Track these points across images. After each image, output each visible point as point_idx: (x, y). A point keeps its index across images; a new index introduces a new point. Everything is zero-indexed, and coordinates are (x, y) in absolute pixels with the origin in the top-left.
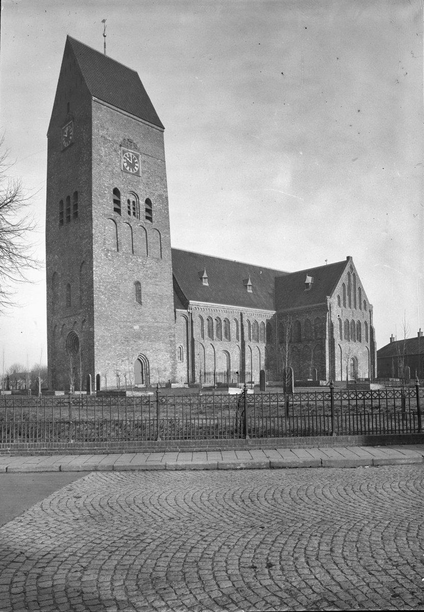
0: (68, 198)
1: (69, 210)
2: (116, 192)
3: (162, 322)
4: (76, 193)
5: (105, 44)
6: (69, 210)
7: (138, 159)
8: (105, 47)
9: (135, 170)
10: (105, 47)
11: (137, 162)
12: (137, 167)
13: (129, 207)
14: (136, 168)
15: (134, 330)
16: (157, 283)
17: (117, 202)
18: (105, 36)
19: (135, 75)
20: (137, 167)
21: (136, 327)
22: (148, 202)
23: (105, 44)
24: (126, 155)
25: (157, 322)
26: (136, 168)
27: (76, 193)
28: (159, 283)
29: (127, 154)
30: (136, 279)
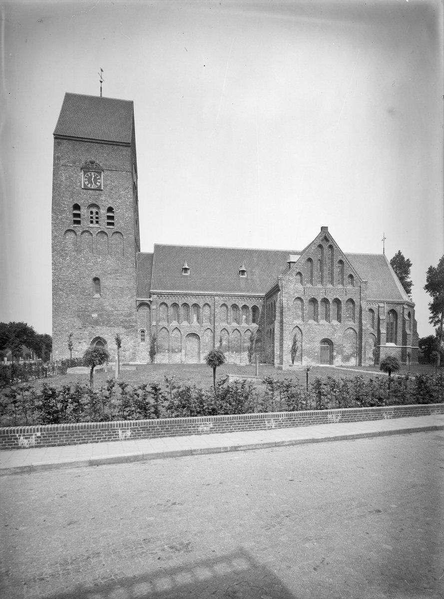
3: (123, 310)
5: (101, 88)
7: (101, 177)
9: (97, 185)
11: (99, 179)
14: (98, 183)
15: (93, 318)
16: (118, 277)
18: (101, 82)
20: (99, 182)
21: (95, 315)
22: (110, 210)
23: (101, 88)
24: (88, 175)
25: (117, 310)
26: (98, 183)
28: (120, 277)
29: (89, 173)
30: (95, 276)
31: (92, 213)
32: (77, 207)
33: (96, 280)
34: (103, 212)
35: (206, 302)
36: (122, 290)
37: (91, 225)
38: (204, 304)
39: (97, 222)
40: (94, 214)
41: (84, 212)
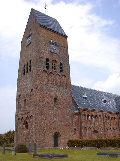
2: (47, 60)
13: (53, 66)
17: (48, 64)
22: (61, 64)
31: (53, 64)
32: (47, 60)
37: (53, 70)
39: (55, 69)
40: (54, 65)
41: (50, 62)
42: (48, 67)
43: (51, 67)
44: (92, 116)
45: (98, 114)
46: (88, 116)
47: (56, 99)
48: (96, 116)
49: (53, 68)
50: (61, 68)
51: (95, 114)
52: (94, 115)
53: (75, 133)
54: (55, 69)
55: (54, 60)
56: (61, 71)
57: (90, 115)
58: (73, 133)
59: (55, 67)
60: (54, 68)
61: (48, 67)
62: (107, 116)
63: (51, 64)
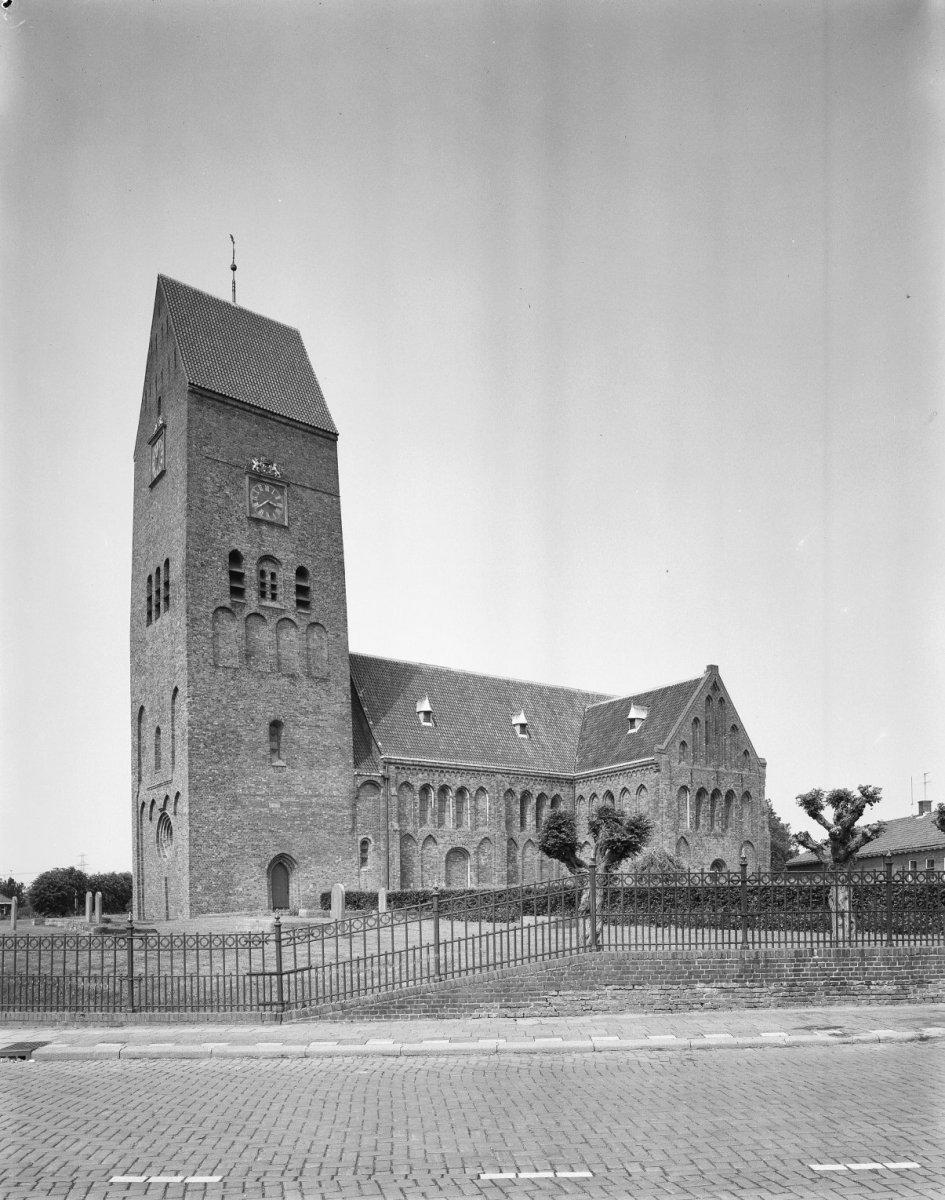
0: (158, 569)
1: (158, 592)
2: (235, 557)
4: (167, 562)
5: (234, 283)
6: (158, 592)
8: (234, 291)
9: (277, 515)
10: (234, 291)
12: (280, 509)
17: (236, 577)
18: (234, 268)
19: (287, 341)
22: (302, 573)
23: (234, 283)
27: (167, 562)
30: (271, 716)
31: (262, 574)
32: (235, 557)
33: (276, 725)
34: (286, 576)
35: (481, 785)
36: (327, 750)
38: (477, 787)
40: (268, 578)
41: (249, 569)
42: (237, 592)
43: (252, 594)
44: (444, 789)
45: (472, 784)
46: (425, 789)
47: (276, 725)
48: (461, 791)
49: (263, 595)
50: (302, 590)
51: (459, 784)
52: (455, 788)
53: (364, 861)
54: (274, 597)
55: (267, 558)
56: (302, 604)
57: (437, 787)
58: (356, 858)
59: (274, 587)
60: (267, 590)
61: (237, 592)
62: (518, 789)
63: (254, 574)
